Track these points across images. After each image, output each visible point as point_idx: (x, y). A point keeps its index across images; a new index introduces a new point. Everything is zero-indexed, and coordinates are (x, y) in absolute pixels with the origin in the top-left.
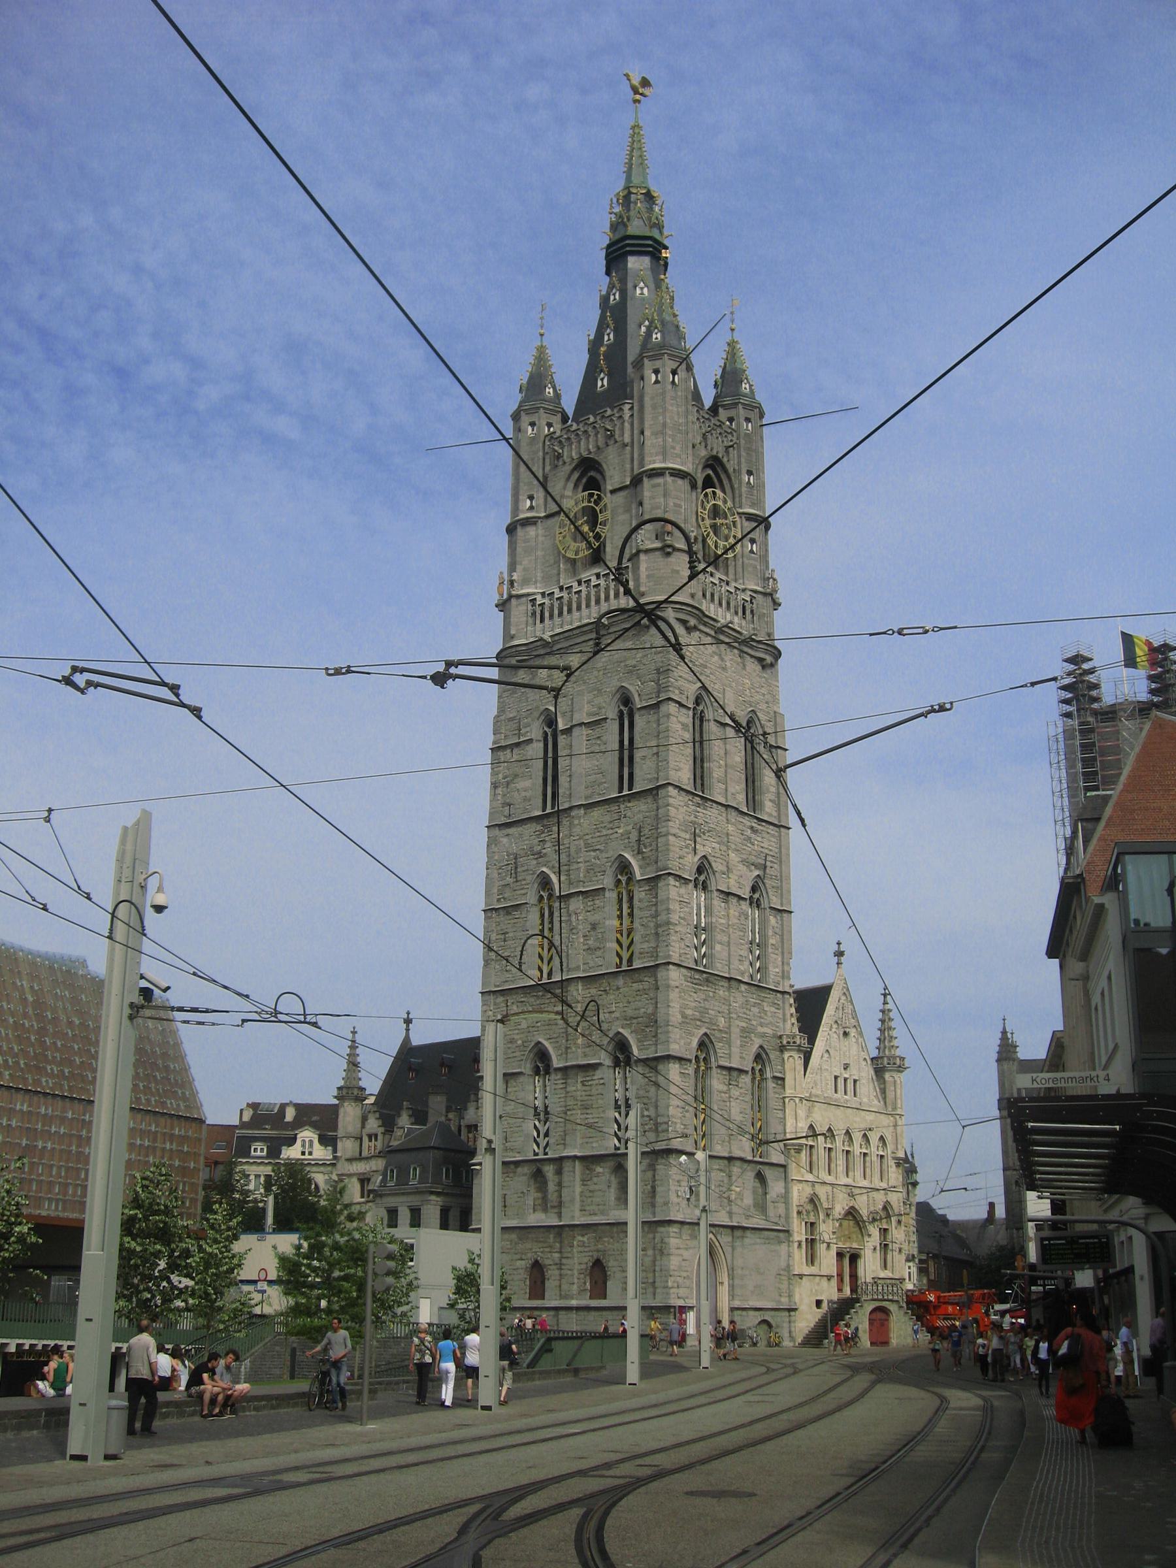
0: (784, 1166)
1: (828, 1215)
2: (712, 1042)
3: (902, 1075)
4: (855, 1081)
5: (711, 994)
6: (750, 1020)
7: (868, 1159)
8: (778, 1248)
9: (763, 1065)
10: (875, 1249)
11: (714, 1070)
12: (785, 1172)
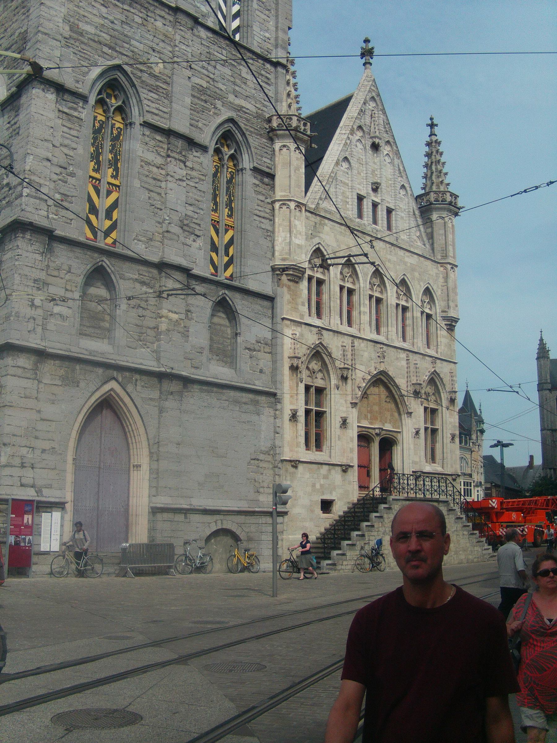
0: (271, 299)
1: (344, 379)
2: (133, 85)
3: (456, 220)
4: (389, 211)
5: (139, 20)
6: (213, 80)
7: (409, 315)
8: (255, 418)
9: (238, 149)
10: (417, 433)
11: (137, 130)
12: (273, 308)
